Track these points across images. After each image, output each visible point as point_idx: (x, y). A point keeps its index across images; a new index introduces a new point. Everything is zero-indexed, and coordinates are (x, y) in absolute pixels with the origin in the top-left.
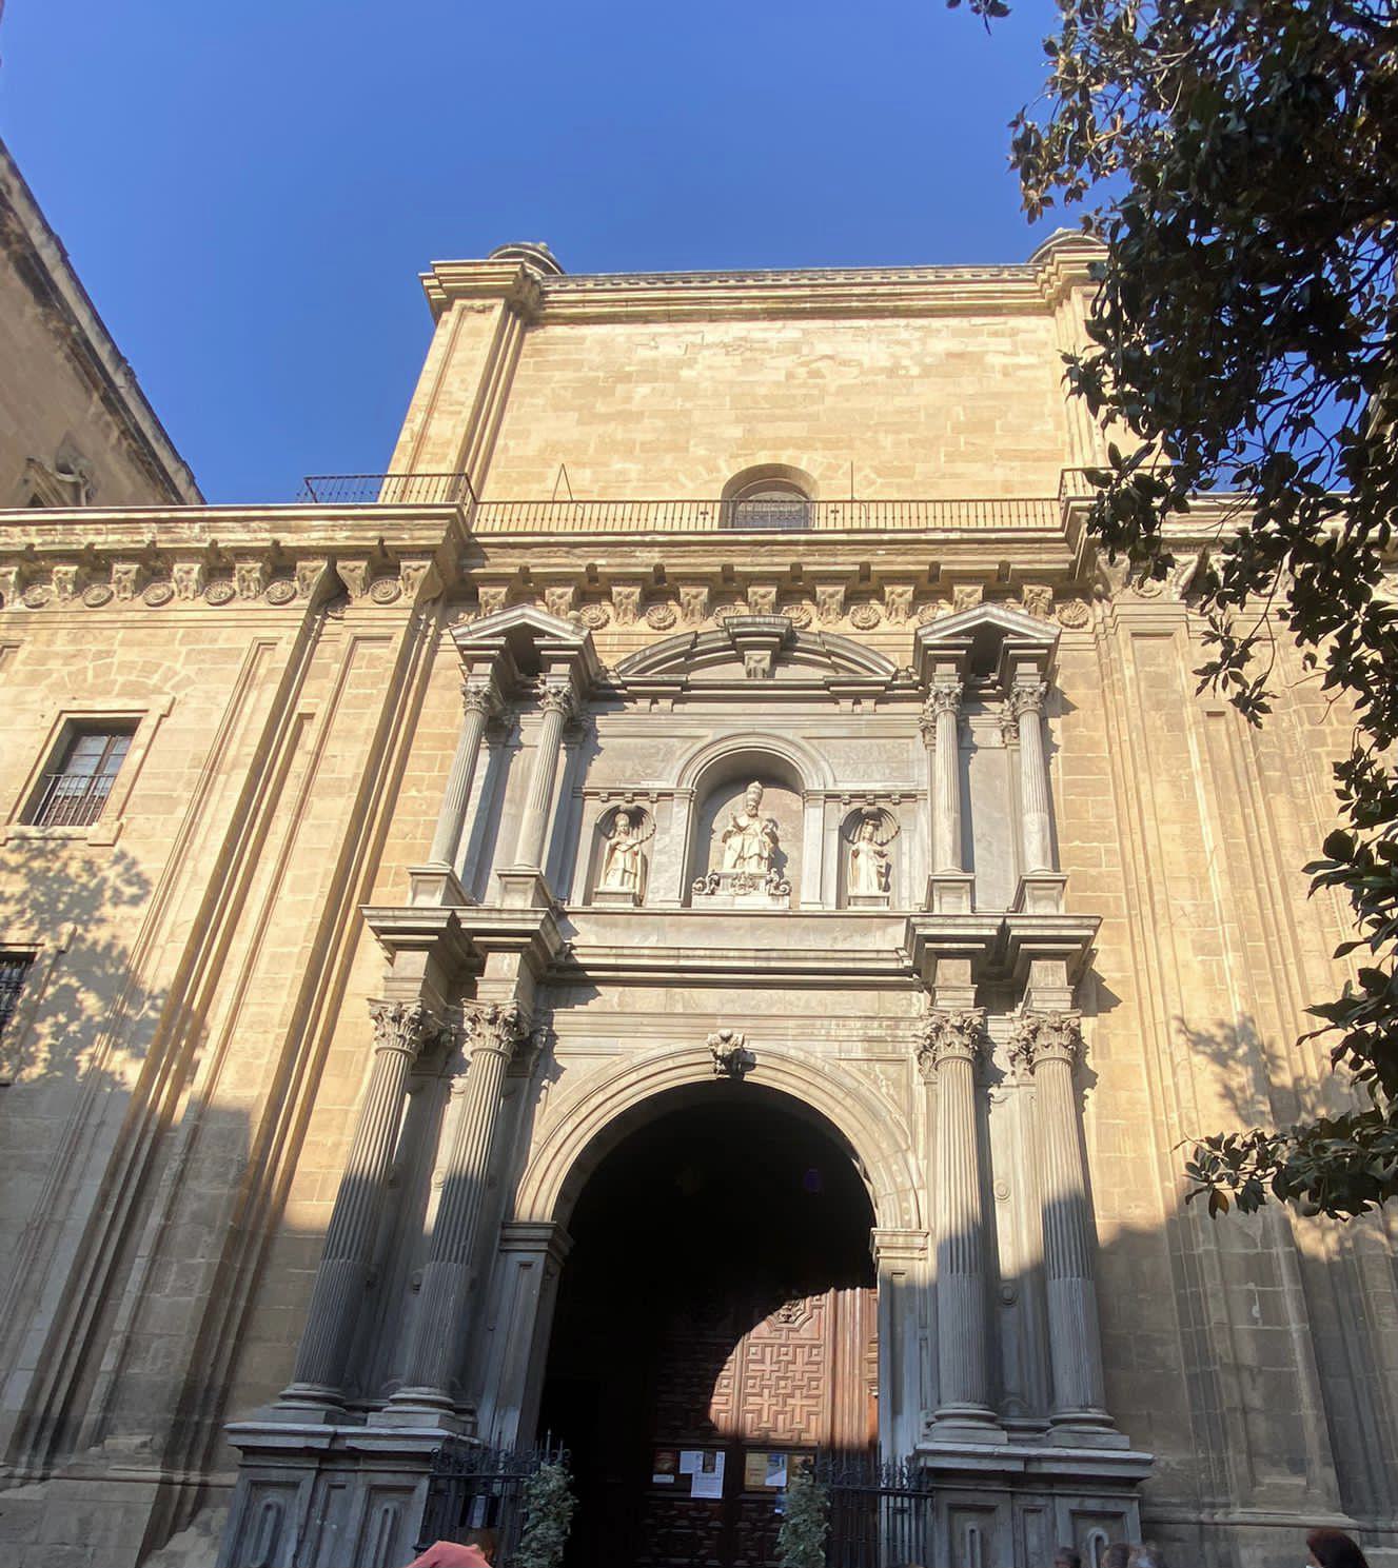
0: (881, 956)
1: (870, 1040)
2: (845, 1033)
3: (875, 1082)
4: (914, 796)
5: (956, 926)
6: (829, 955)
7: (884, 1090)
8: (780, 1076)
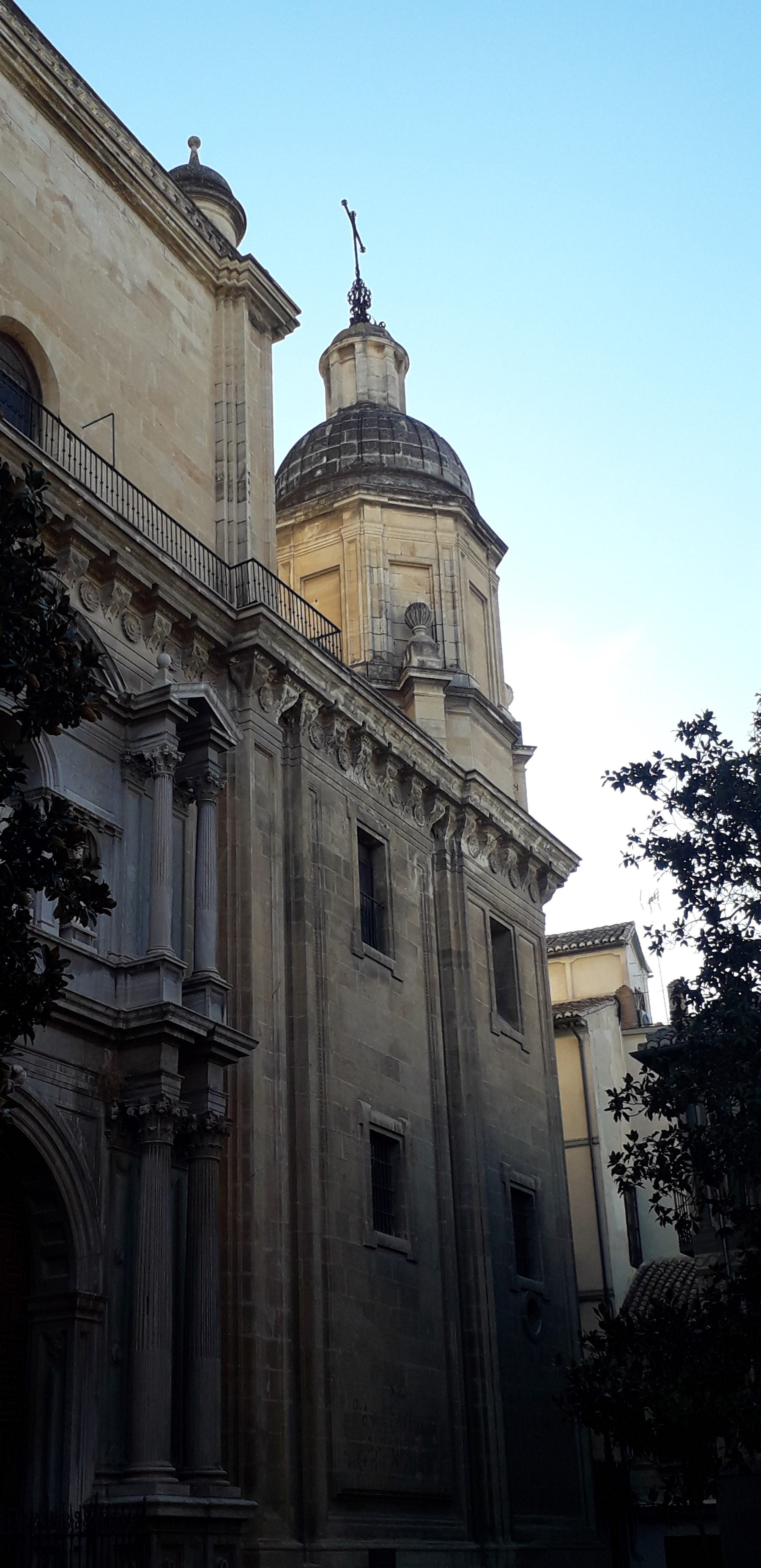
0: (109, 1012)
1: (78, 1091)
2: (64, 1079)
3: (76, 1136)
4: (114, 830)
5: (190, 1021)
6: (77, 999)
7: (81, 1144)
8: (23, 1116)
